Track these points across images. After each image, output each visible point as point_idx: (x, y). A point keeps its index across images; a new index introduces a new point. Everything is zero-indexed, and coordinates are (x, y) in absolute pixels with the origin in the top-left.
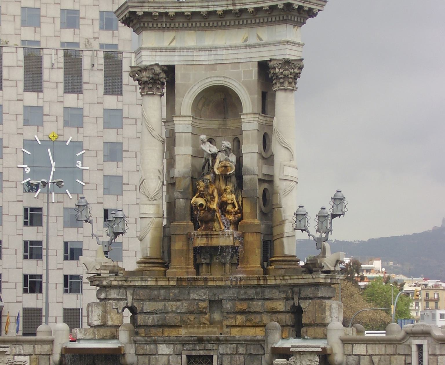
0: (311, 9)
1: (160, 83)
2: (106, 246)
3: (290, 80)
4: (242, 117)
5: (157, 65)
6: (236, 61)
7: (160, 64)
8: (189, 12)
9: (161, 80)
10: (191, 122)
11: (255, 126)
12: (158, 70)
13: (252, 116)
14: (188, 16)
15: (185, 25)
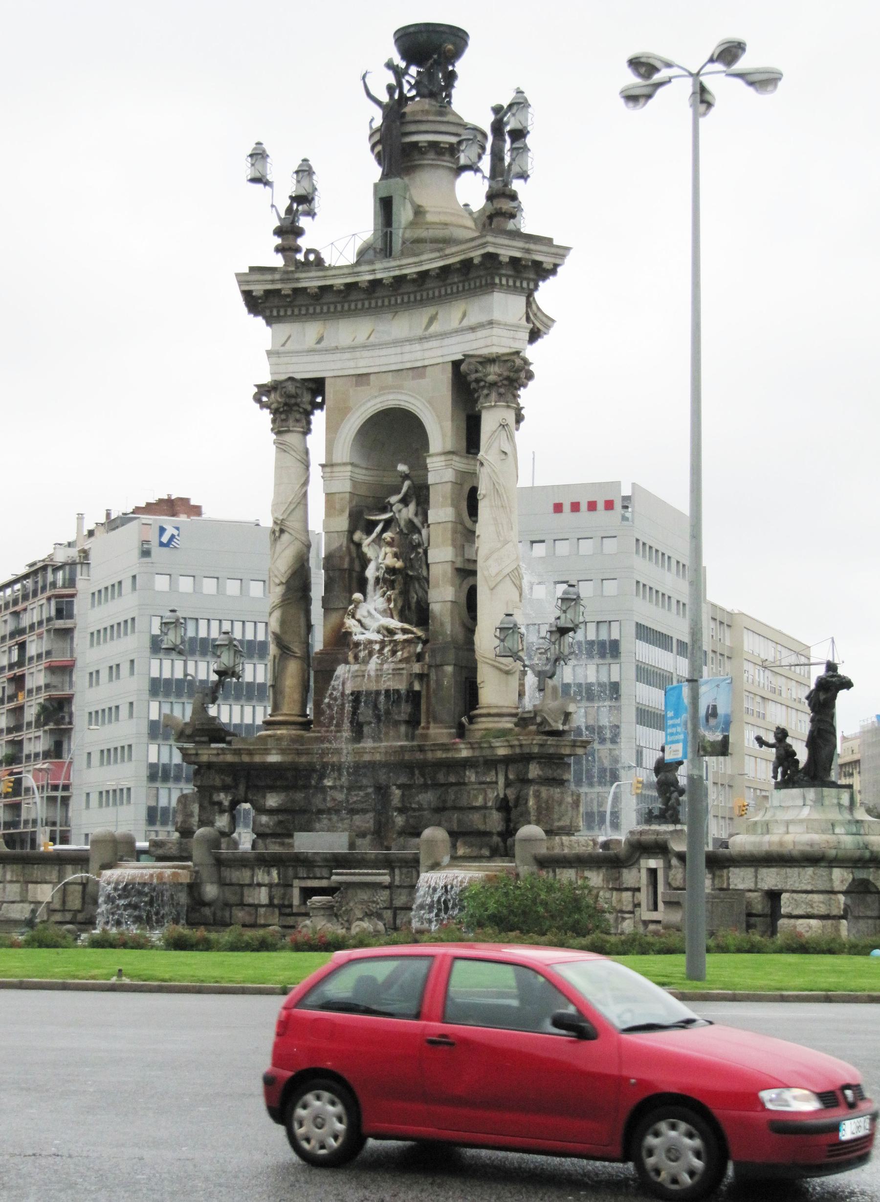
0: (537, 264)
1: (301, 410)
2: (207, 695)
3: (502, 390)
4: (428, 460)
5: (291, 379)
6: (419, 364)
7: (298, 376)
8: (341, 284)
9: (304, 406)
10: (349, 474)
11: (449, 475)
12: (291, 388)
13: (443, 458)
14: (340, 291)
15: (339, 308)
